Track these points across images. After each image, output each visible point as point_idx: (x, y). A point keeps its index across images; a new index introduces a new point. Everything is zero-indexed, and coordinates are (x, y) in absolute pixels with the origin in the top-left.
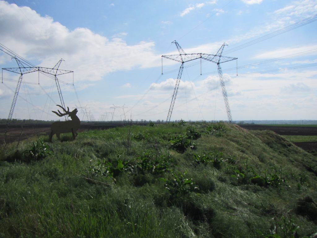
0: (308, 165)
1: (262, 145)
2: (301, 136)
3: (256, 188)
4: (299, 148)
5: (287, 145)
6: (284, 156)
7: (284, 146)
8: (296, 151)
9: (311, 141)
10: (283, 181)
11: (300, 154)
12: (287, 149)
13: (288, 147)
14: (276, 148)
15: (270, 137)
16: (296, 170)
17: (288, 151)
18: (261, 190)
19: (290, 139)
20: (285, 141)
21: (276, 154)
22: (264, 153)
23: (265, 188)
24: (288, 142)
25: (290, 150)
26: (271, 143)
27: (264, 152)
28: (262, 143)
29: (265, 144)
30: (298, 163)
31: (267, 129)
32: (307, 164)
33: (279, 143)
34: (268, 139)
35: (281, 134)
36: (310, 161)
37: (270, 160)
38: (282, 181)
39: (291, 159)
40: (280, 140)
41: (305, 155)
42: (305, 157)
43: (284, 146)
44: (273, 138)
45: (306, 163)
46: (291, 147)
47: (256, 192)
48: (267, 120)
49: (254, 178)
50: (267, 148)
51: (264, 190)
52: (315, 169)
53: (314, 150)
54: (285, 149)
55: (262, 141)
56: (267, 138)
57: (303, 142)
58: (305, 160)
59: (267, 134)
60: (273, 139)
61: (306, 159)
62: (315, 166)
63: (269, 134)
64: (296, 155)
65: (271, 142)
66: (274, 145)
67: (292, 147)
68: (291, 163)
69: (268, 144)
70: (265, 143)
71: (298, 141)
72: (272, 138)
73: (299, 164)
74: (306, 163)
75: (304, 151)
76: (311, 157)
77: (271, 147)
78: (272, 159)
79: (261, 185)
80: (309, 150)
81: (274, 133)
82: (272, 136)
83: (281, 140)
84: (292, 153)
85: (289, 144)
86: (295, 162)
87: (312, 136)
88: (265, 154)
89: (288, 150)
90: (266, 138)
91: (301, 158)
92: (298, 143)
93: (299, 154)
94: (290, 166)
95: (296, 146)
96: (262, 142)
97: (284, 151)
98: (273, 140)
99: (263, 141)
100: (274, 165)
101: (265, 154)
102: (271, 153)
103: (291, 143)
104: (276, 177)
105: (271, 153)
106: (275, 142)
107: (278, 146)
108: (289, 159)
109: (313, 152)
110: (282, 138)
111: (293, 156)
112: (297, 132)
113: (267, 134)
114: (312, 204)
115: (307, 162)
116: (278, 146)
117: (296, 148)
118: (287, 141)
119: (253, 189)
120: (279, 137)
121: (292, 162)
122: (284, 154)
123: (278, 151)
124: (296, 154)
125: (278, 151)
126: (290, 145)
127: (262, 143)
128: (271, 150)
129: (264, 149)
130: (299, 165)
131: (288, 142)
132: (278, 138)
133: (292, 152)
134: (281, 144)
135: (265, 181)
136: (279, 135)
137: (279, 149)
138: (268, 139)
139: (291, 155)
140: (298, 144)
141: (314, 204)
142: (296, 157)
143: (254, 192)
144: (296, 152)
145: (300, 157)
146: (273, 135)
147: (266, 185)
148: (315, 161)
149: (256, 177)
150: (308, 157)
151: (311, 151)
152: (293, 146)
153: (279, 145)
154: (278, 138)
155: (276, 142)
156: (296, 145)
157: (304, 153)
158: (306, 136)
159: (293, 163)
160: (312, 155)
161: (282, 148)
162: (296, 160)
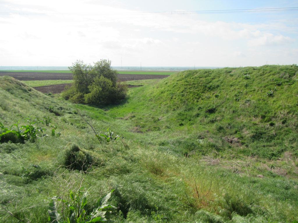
0: (49, 107)
1: (3, 92)
2: (38, 81)
3: (10, 147)
4: (39, 92)
5: (27, 90)
6: (26, 101)
7: (25, 91)
8: (36, 95)
9: (46, 85)
10: (39, 130)
11: (41, 98)
12: (28, 94)
13: (29, 92)
14: (17, 94)
15: (9, 83)
16: (41, 114)
17: (29, 96)
18: (16, 149)
19: (30, 84)
20: (25, 86)
21: (18, 100)
22: (6, 100)
23: (21, 144)
24: (28, 87)
25: (31, 95)
26: (11, 89)
27: (6, 99)
28: (2, 89)
29: (5, 91)
30: (39, 106)
31: (6, 75)
32: (47, 106)
33: (19, 89)
34: (7, 84)
35: (21, 79)
36: (49, 103)
37: (14, 107)
38: (38, 131)
39: (33, 103)
40: (20, 85)
41: (45, 98)
42: (45, 100)
43: (25, 91)
44: (13, 84)
45: (47, 105)
46: (32, 92)
47: (10, 153)
48: (2, 66)
49: (4, 134)
50: (8, 95)
51: (21, 147)
52: (54, 110)
53: (50, 93)
54: (26, 94)
55: (1, 88)
56: (6, 84)
57: (41, 86)
58: (46, 103)
59: (5, 80)
60: (13, 85)
61: (46, 101)
62: (54, 107)
63: (8, 80)
64: (37, 99)
65: (11, 88)
66: (14, 91)
67: (33, 91)
68: (34, 107)
69: (8, 90)
70: (5, 90)
71: (35, 85)
72: (11, 84)
73: (41, 107)
74: (47, 105)
75: (43, 94)
76: (50, 100)
77: (12, 94)
78: (15, 106)
79: (14, 141)
80: (46, 93)
81: (13, 79)
82: (11, 82)
83: (21, 85)
84: (33, 98)
85: (29, 89)
86: (37, 105)
87: (47, 81)
88: (7, 101)
89: (29, 95)
90: (5, 85)
91: (42, 101)
92: (38, 87)
93: (39, 97)
94: (34, 110)
95: (36, 91)
96: (1, 89)
97: (25, 96)
98: (13, 86)
99: (2, 88)
100: (19, 112)
101: (7, 101)
102: (13, 100)
103: (31, 88)
104: (31, 128)
105: (13, 100)
106: (15, 88)
107: (19, 92)
108: (31, 104)
109: (50, 95)
110: (22, 84)
111: (34, 100)
112: (34, 77)
113: (5, 80)
114: (79, 153)
115: (47, 104)
116: (19, 92)
117: (37, 92)
118: (27, 86)
119: (5, 149)
120: (19, 82)
121: (34, 106)
122: (26, 99)
123: (20, 96)
124: (37, 98)
125: (20, 96)
126: (30, 90)
127: (2, 89)
128: (13, 96)
129: (5, 96)
130: (41, 108)
131: (28, 87)
132: (17, 84)
133: (33, 96)
134: (22, 89)
135: (18, 135)
136: (19, 81)
137: (20, 95)
138: (7, 84)
139: (32, 99)
140: (36, 88)
141: (81, 152)
142: (37, 100)
143: (8, 153)
144: (37, 96)
145: (40, 101)
146: (12, 81)
147: (22, 140)
148: (53, 103)
149: (7, 132)
150: (47, 99)
151: (48, 94)
152: (33, 90)
153: (20, 91)
154: (17, 84)
155: (16, 87)
156: (36, 90)
157: (43, 97)
158: (42, 81)
159: (35, 107)
160: (51, 98)
161: (23, 93)
162: (38, 104)
